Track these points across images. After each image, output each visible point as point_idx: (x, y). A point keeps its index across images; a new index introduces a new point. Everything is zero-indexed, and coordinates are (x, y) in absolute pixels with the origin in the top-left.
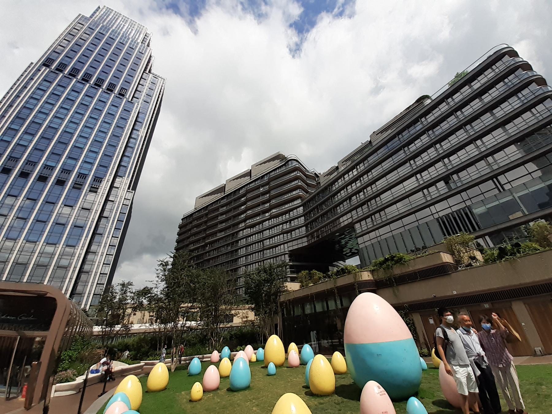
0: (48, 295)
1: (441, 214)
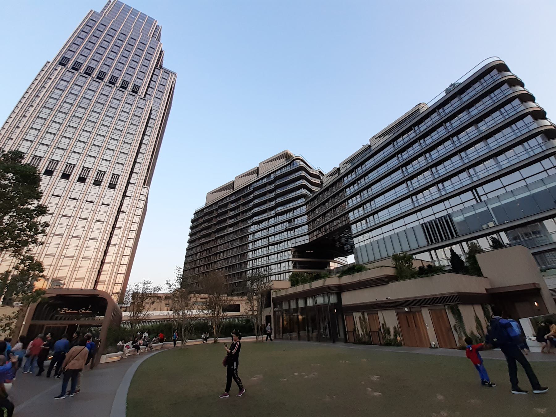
0: (100, 296)
1: (426, 220)
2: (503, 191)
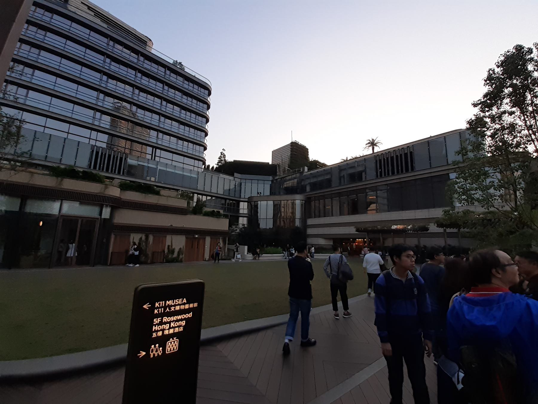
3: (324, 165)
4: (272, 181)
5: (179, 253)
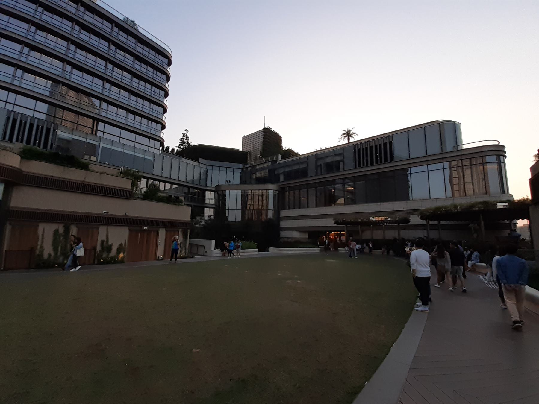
2: (117, 139)
3: (297, 154)
4: (242, 169)
5: (119, 251)
